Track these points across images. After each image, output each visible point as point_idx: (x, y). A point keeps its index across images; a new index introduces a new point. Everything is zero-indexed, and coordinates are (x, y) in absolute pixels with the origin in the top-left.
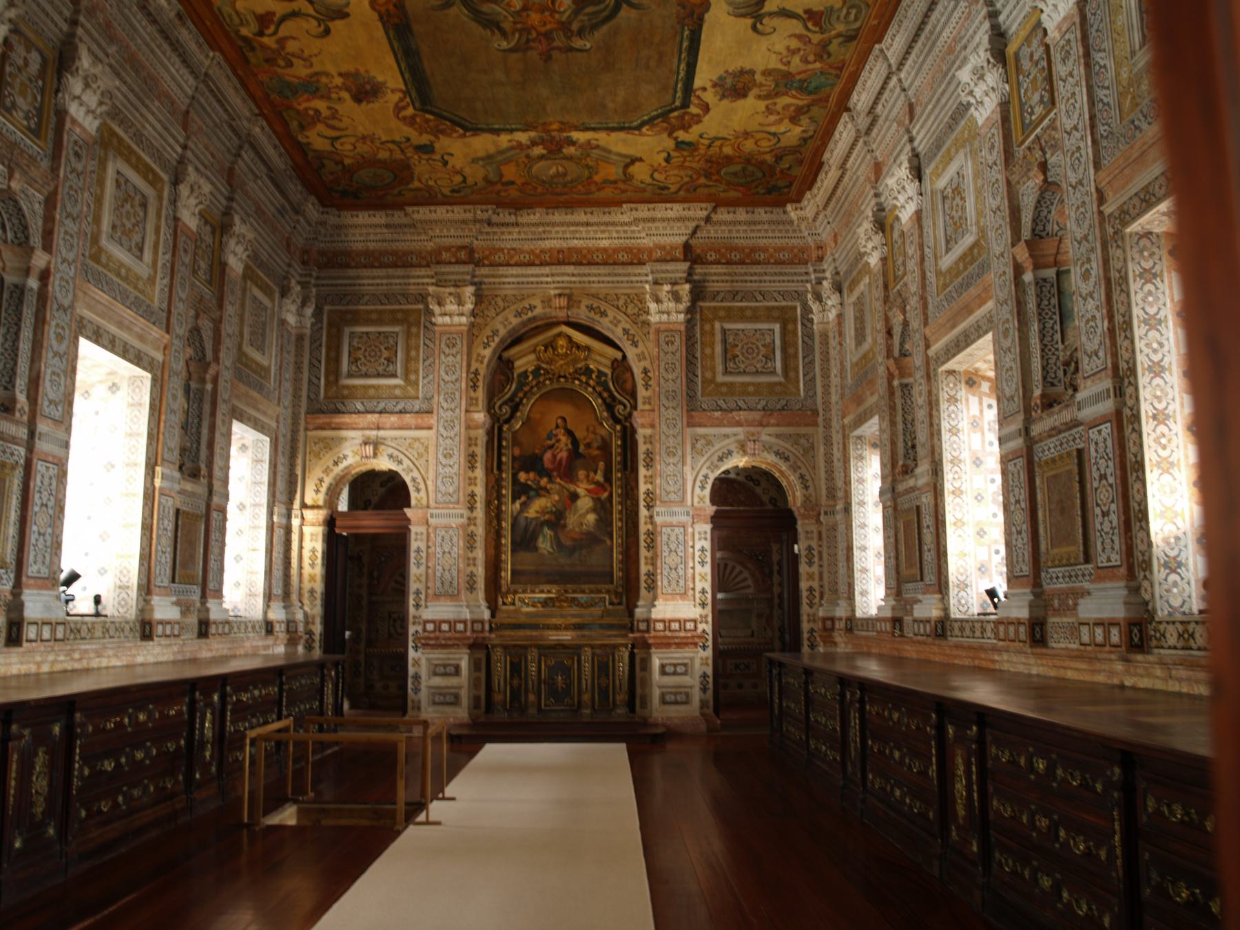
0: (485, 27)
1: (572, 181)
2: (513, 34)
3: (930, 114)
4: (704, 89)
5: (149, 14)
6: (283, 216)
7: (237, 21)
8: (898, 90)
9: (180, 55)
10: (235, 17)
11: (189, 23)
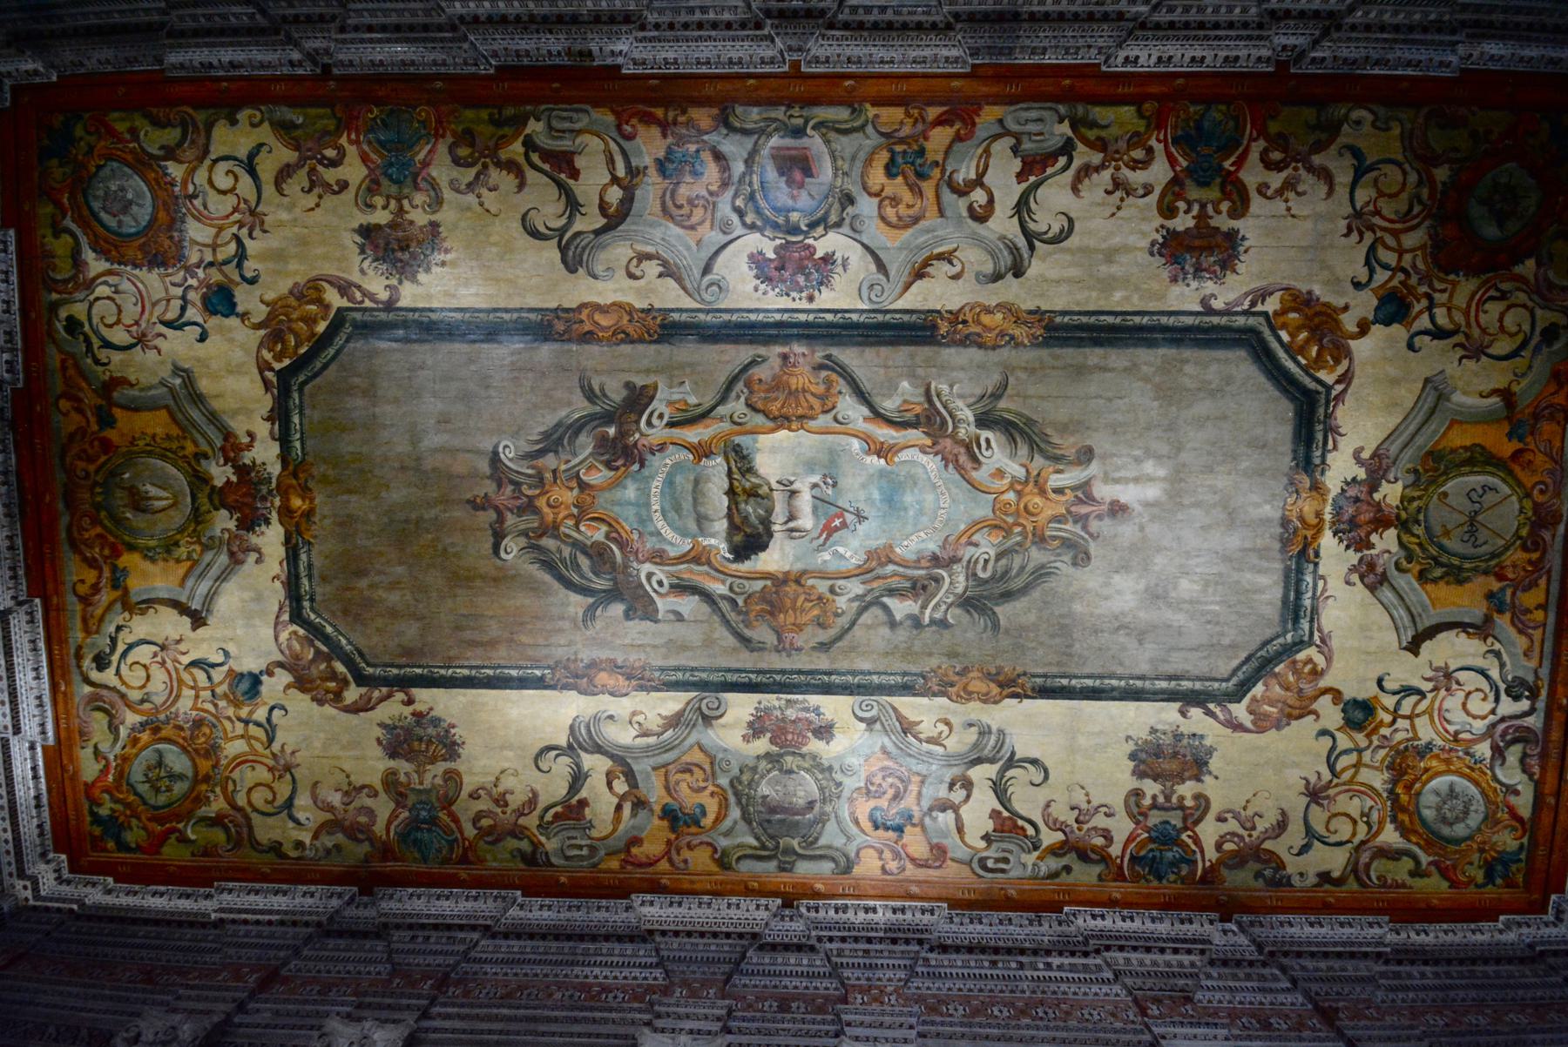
0: (546, 435)
1: (118, 521)
2: (532, 467)
3: (497, 1018)
4: (410, 702)
8: (462, 948)
9: (518, 18)
10: (567, 125)
11: (566, 61)
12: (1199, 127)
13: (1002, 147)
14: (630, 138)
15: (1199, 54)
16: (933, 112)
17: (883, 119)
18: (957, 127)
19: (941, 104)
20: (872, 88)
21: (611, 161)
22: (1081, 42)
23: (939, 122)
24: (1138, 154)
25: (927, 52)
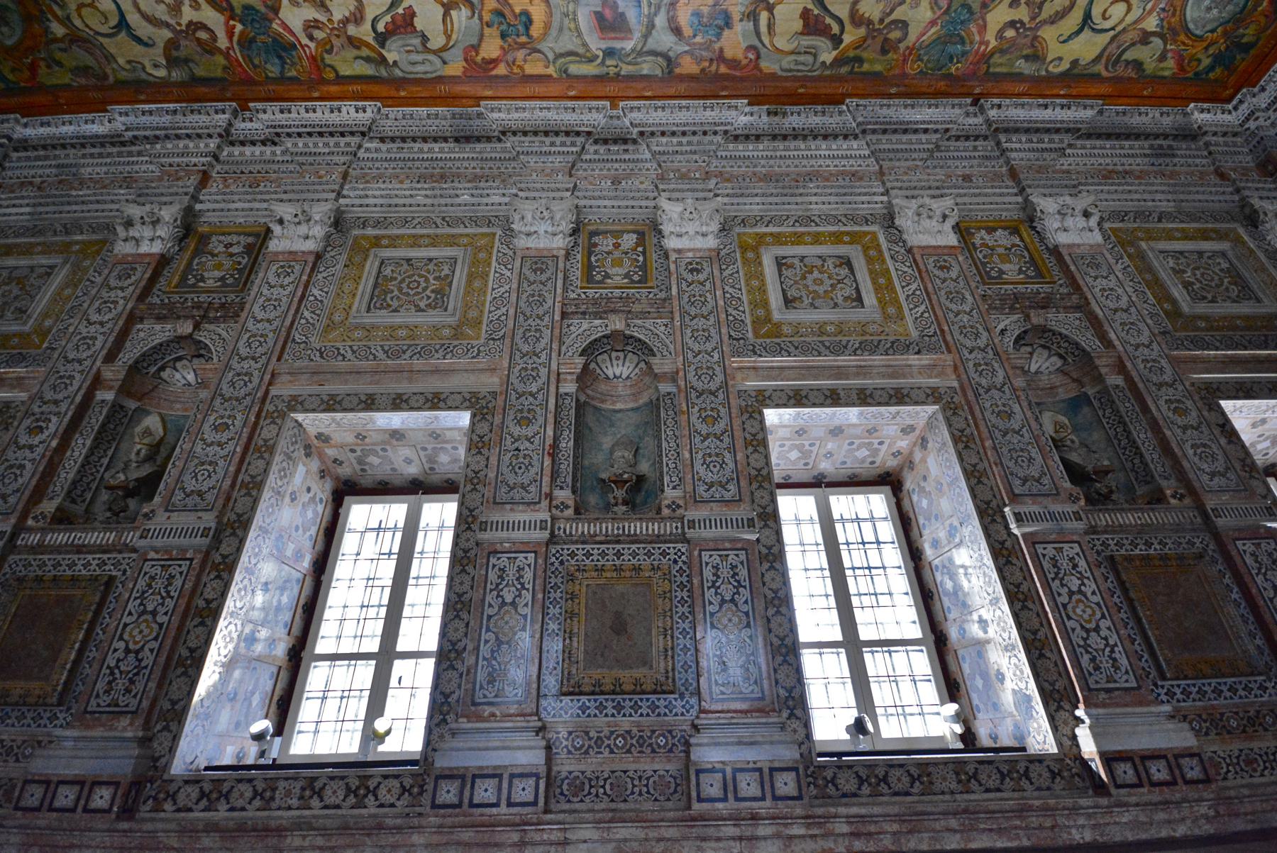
5: (747, 137)
6: (1174, 156)
7: (810, 59)
9: (815, 138)
10: (802, 58)
12: (280, 57)
13: (437, 41)
14: (751, 48)
15: (311, 115)
16: (501, 70)
17: (541, 64)
18: (479, 59)
19: (497, 76)
20: (554, 89)
21: (770, 27)
22: (404, 123)
23: (495, 62)
24: (319, 35)
25: (516, 115)
